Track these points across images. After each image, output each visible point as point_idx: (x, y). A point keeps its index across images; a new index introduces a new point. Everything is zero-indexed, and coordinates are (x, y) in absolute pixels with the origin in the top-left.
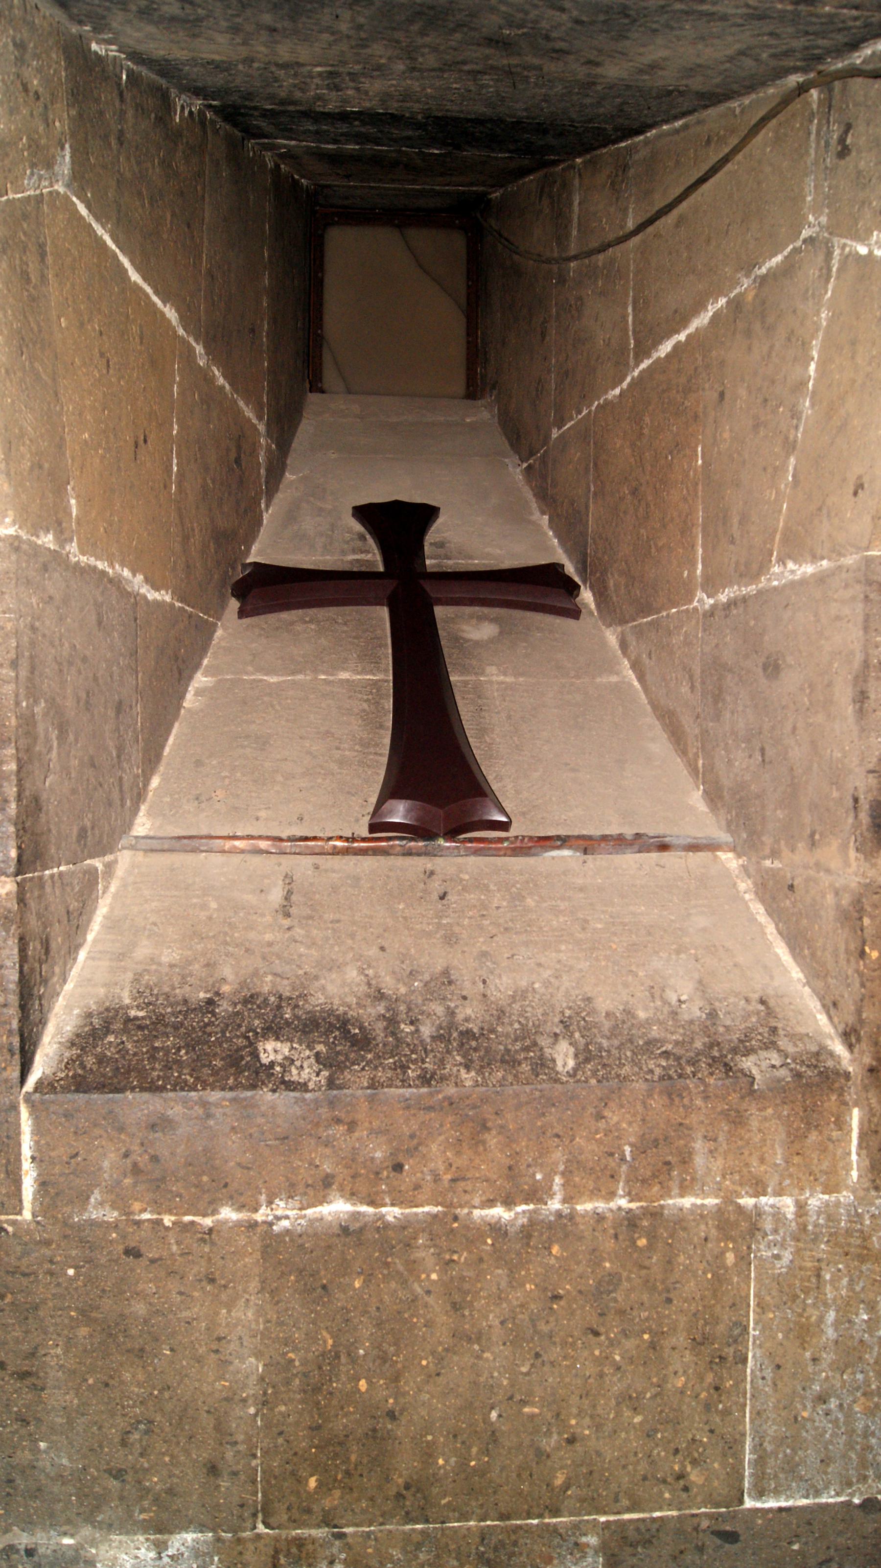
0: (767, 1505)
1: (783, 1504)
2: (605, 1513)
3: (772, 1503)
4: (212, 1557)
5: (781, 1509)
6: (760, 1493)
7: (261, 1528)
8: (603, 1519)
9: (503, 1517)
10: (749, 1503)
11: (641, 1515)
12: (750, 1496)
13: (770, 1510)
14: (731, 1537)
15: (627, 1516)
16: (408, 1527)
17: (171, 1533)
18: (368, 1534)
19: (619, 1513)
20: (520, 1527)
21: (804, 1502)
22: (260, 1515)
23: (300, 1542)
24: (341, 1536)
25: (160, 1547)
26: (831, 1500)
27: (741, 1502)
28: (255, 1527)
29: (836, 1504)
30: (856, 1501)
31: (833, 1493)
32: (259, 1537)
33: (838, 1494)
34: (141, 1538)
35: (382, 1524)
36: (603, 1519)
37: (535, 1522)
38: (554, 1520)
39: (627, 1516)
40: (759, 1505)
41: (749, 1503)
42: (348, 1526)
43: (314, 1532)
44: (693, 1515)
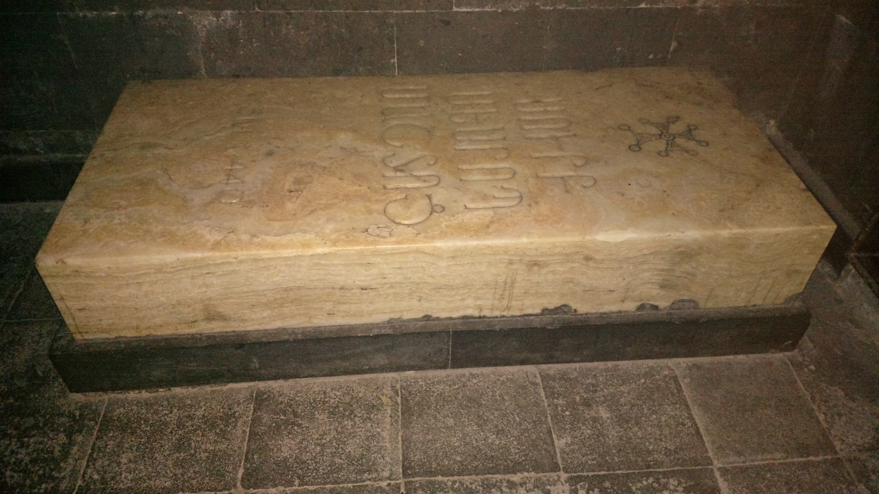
0: (462, 10)
1: (469, 10)
2: (396, 10)
3: (464, 10)
4: (239, 21)
5: (468, 12)
6: (459, 6)
7: (257, 9)
8: (395, 12)
9: (355, 9)
10: (455, 9)
11: (411, 11)
12: (455, 6)
13: (464, 12)
14: (448, 23)
15: (405, 11)
16: (317, 11)
17: (222, 10)
18: (301, 13)
19: (402, 10)
20: (362, 14)
21: (477, 10)
22: (256, 4)
23: (273, 16)
24: (290, 14)
25: (218, 17)
26: (488, 10)
27: (452, 8)
28: (254, 9)
29: (491, 11)
30: (500, 11)
31: (490, 6)
32: (258, 13)
33: (492, 8)
34: (210, 12)
35: (305, 10)
36: (395, 12)
37: (368, 12)
38: (375, 11)
39: (405, 11)
40: (459, 10)
41: (455, 9)
42: (293, 10)
43: (279, 12)
44: (433, 13)
